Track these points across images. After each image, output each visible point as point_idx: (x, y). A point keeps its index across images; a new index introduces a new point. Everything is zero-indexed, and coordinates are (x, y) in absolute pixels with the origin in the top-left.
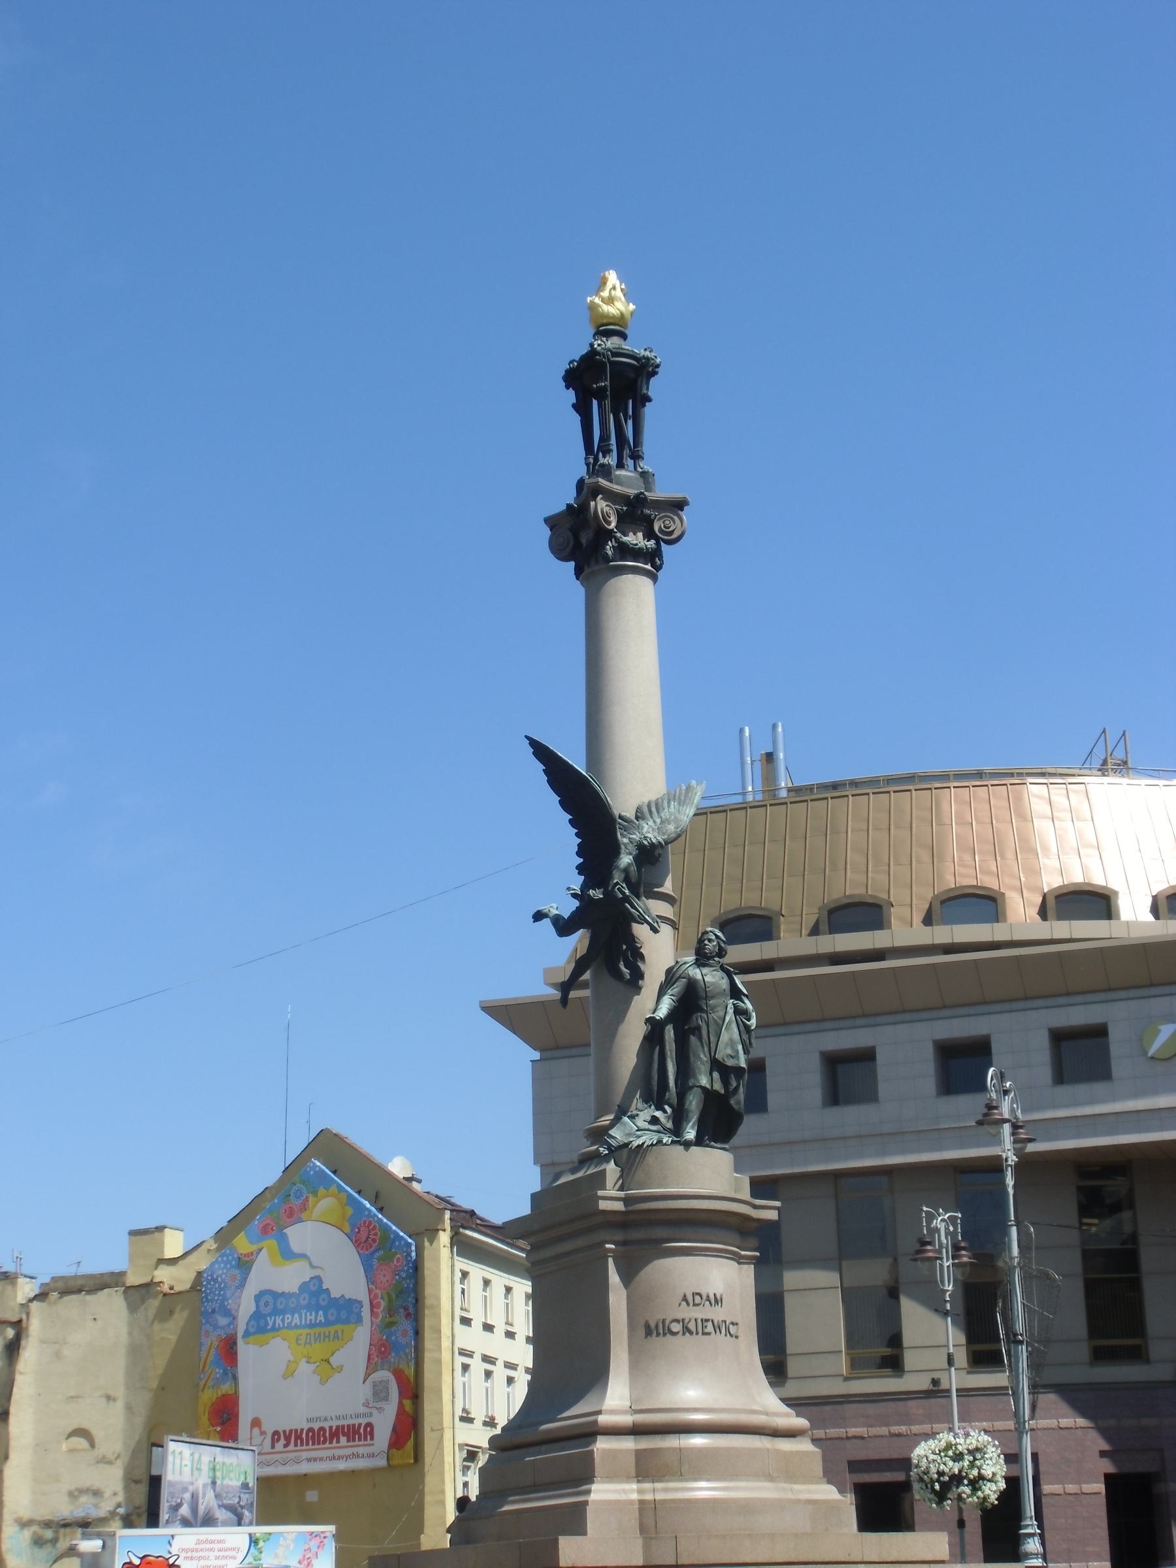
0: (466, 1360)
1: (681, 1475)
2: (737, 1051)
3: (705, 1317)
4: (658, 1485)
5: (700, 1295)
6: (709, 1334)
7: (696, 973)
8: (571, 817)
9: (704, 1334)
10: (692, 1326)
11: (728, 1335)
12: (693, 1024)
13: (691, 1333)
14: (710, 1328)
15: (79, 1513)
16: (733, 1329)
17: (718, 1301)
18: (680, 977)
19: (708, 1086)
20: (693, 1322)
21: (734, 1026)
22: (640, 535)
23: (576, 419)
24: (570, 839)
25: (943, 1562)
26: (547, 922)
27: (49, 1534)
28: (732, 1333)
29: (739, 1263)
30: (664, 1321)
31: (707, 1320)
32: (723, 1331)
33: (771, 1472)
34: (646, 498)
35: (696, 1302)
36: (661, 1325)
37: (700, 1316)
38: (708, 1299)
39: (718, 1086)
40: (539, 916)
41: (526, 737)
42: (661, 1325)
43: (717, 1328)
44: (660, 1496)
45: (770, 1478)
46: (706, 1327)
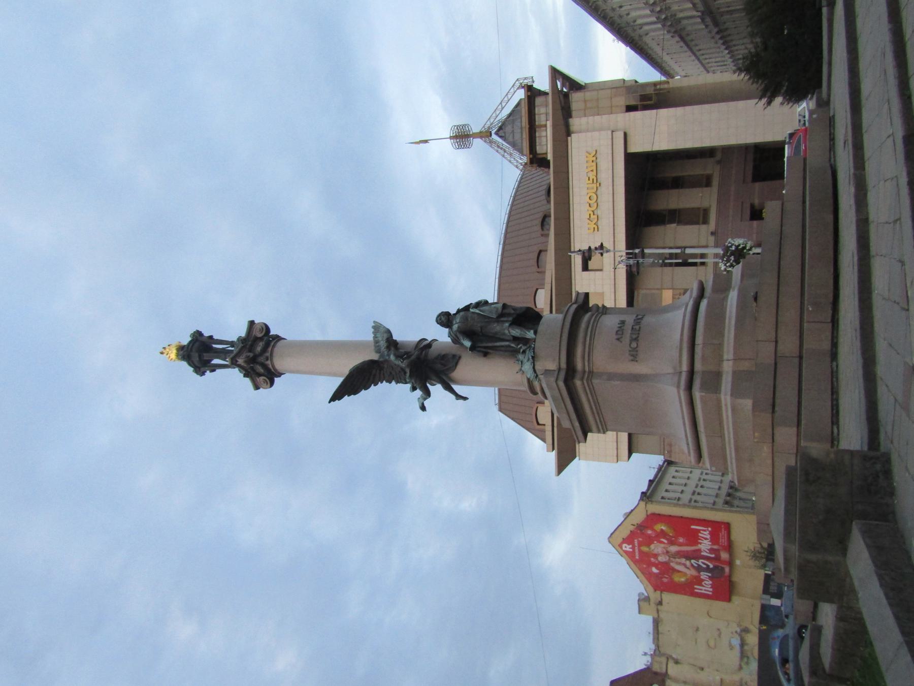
0: (693, 501)
1: (720, 344)
2: (495, 307)
3: (630, 330)
4: (725, 357)
5: (617, 332)
6: (640, 328)
7: (455, 327)
8: (373, 385)
9: (639, 330)
10: (634, 336)
12: (479, 329)
13: (638, 337)
14: (637, 327)
15: (738, 648)
16: (640, 317)
17: (623, 322)
18: (456, 336)
19: (510, 323)
21: (481, 309)
23: (218, 371)
24: (383, 386)
25: (783, 204)
26: (426, 403)
27: (745, 660)
30: (630, 351)
31: (632, 328)
35: (621, 333)
36: (632, 353)
38: (620, 327)
39: (511, 319)
40: (423, 408)
41: (330, 402)
42: (632, 353)
44: (731, 356)
46: (636, 329)
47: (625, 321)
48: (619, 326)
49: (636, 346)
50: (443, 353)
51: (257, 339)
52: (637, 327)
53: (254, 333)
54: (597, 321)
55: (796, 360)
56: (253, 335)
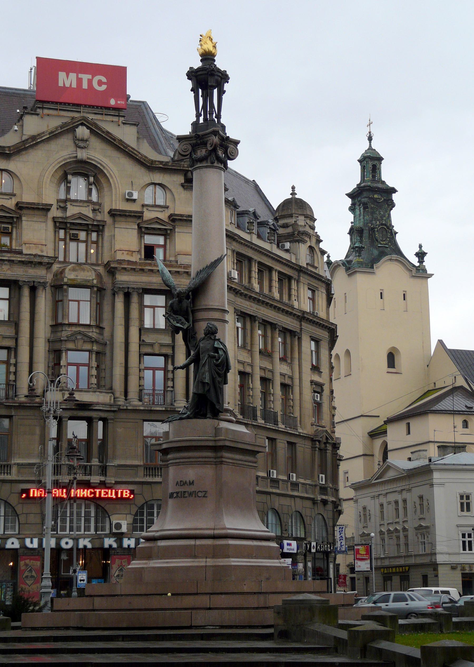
3: (184, 491)
9: (184, 497)
10: (179, 495)
11: (196, 496)
17: (192, 483)
19: (196, 392)
20: (180, 493)
22: (204, 151)
28: (200, 496)
29: (216, 464)
31: (185, 492)
32: (194, 495)
33: (196, 554)
34: (198, 135)
37: (183, 490)
39: (200, 392)
43: (191, 494)
45: (195, 557)
47: (193, 485)
48: (188, 481)
49: (174, 497)
50: (197, 335)
51: (204, 144)
52: (186, 495)
53: (208, 139)
54: (191, 463)
55: (91, 608)
56: (206, 140)
